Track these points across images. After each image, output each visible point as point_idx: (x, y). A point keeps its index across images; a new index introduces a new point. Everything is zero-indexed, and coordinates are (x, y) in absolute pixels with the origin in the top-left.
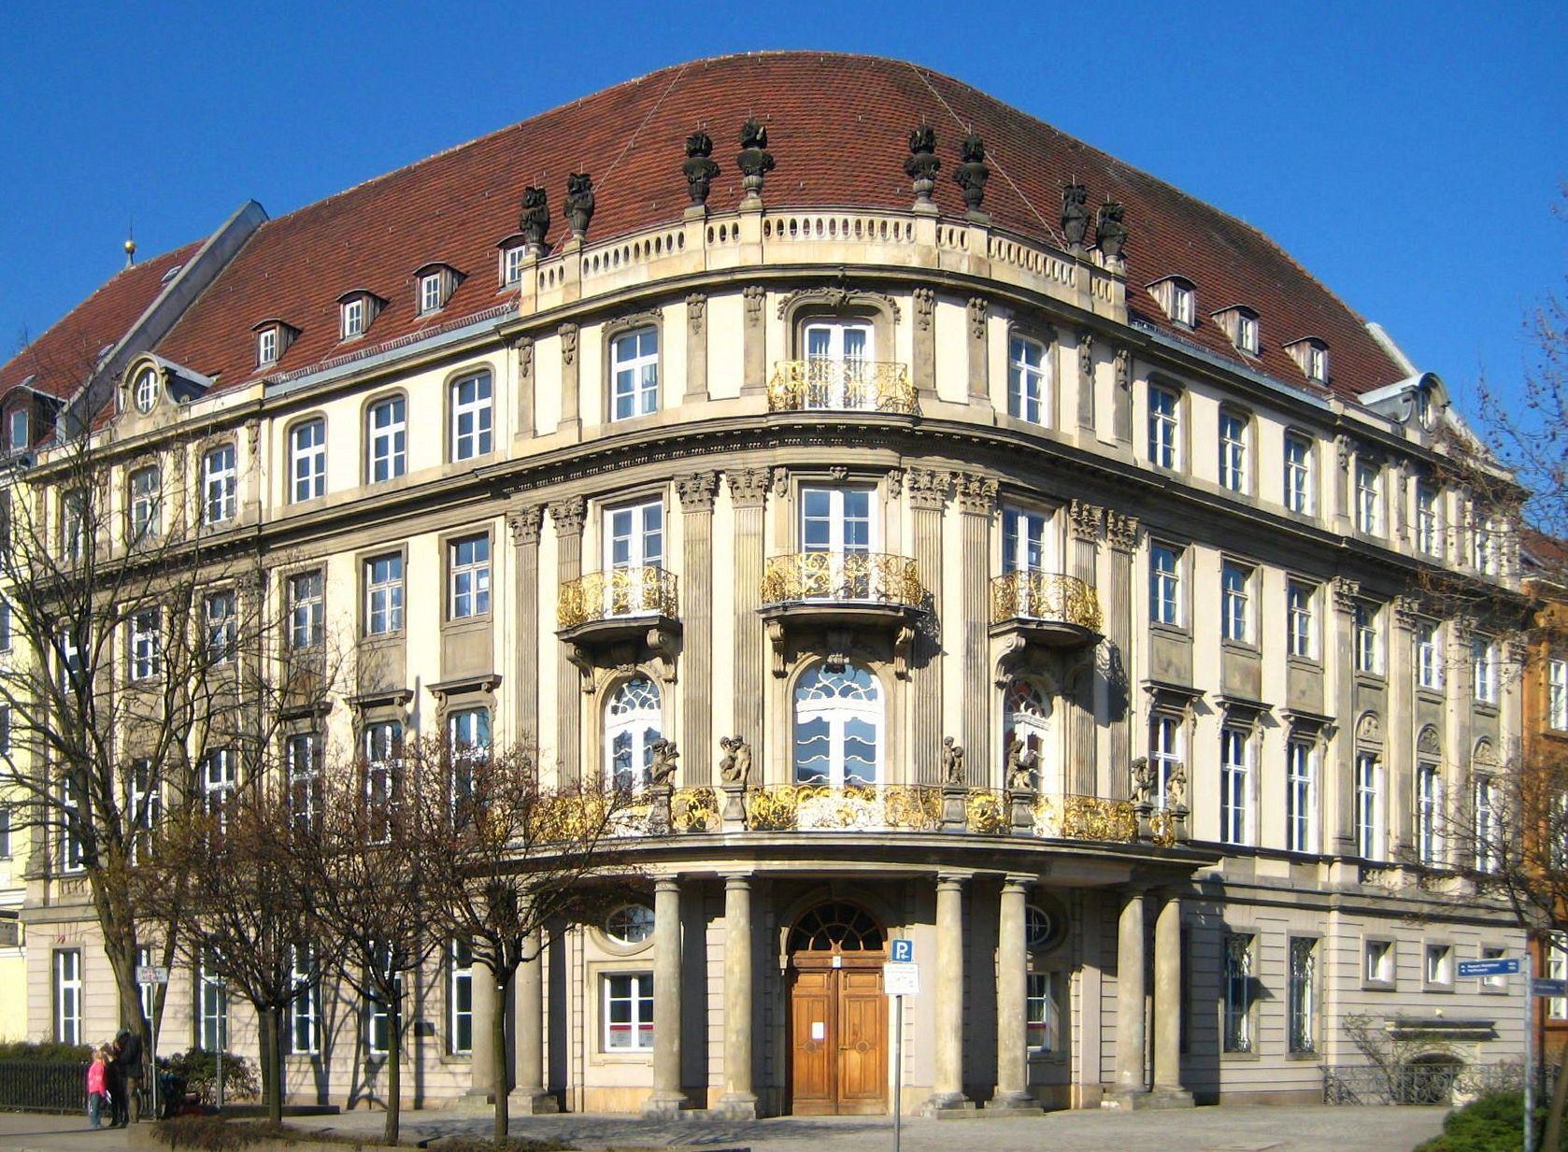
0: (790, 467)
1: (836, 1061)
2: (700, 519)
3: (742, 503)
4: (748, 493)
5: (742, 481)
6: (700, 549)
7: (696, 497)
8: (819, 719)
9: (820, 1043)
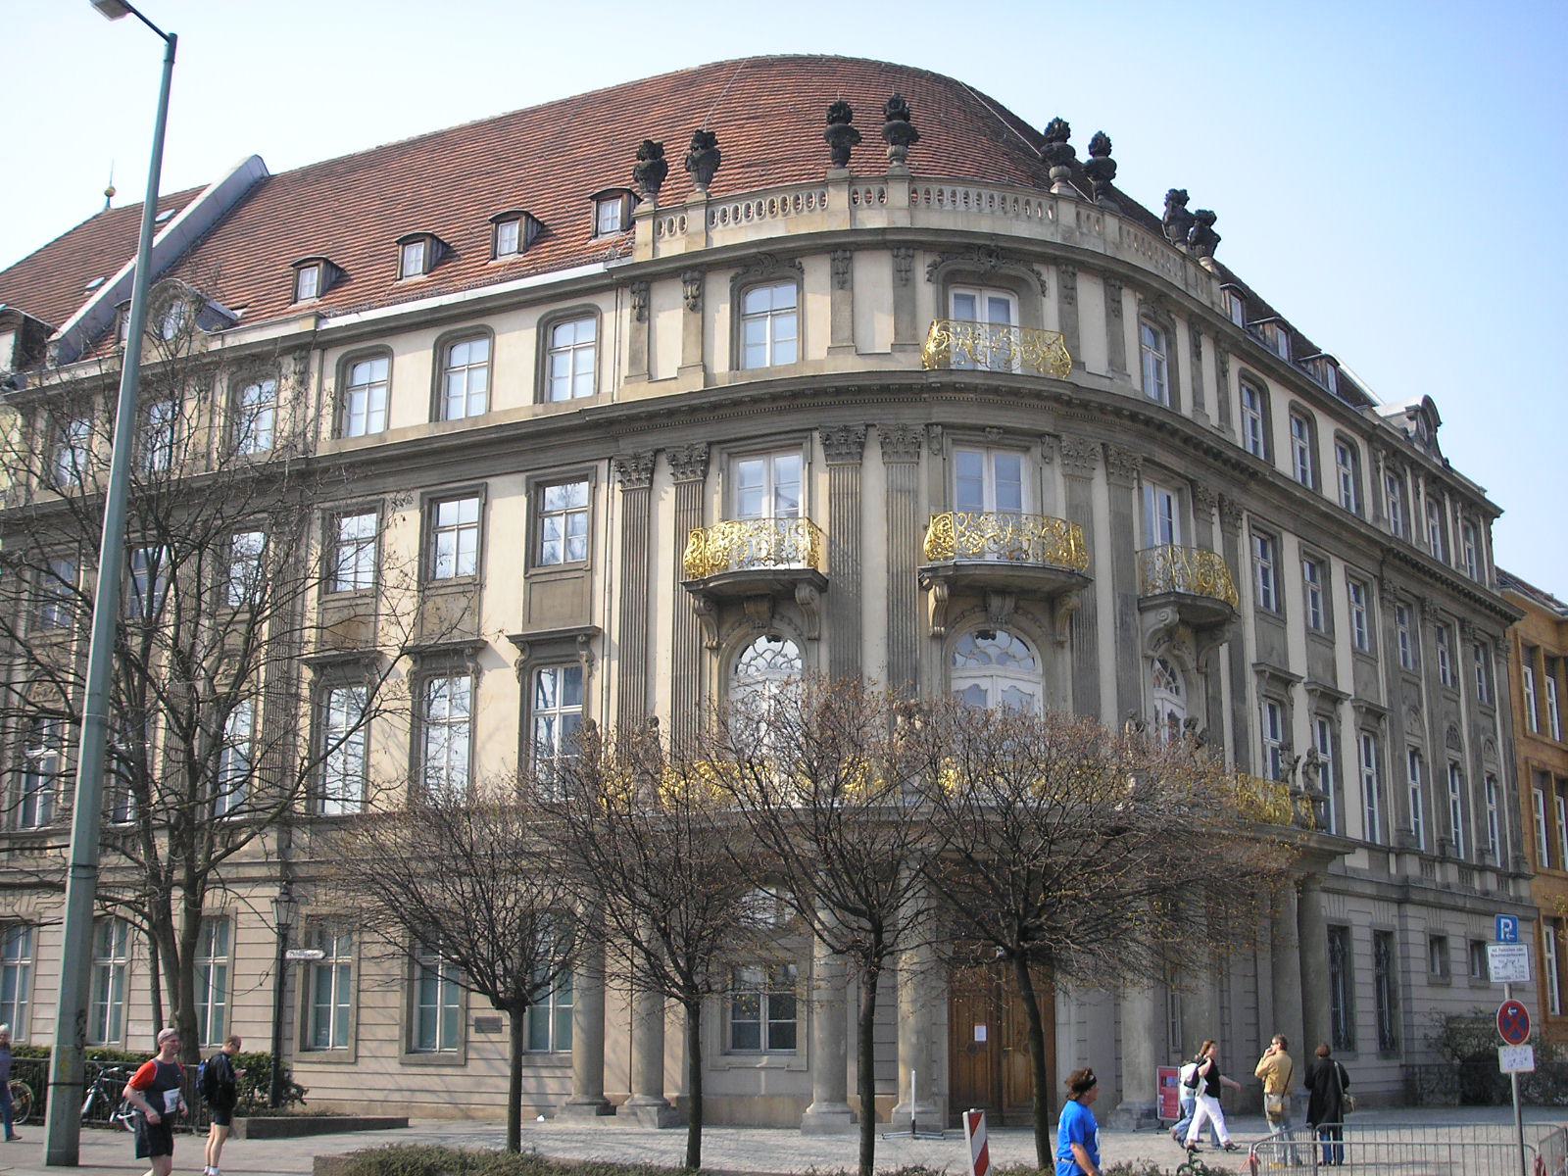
0: (944, 426)
1: (999, 1064)
2: (847, 477)
3: (895, 458)
4: (901, 448)
5: (895, 436)
6: (848, 503)
7: (844, 450)
8: (977, 686)
9: (981, 1043)
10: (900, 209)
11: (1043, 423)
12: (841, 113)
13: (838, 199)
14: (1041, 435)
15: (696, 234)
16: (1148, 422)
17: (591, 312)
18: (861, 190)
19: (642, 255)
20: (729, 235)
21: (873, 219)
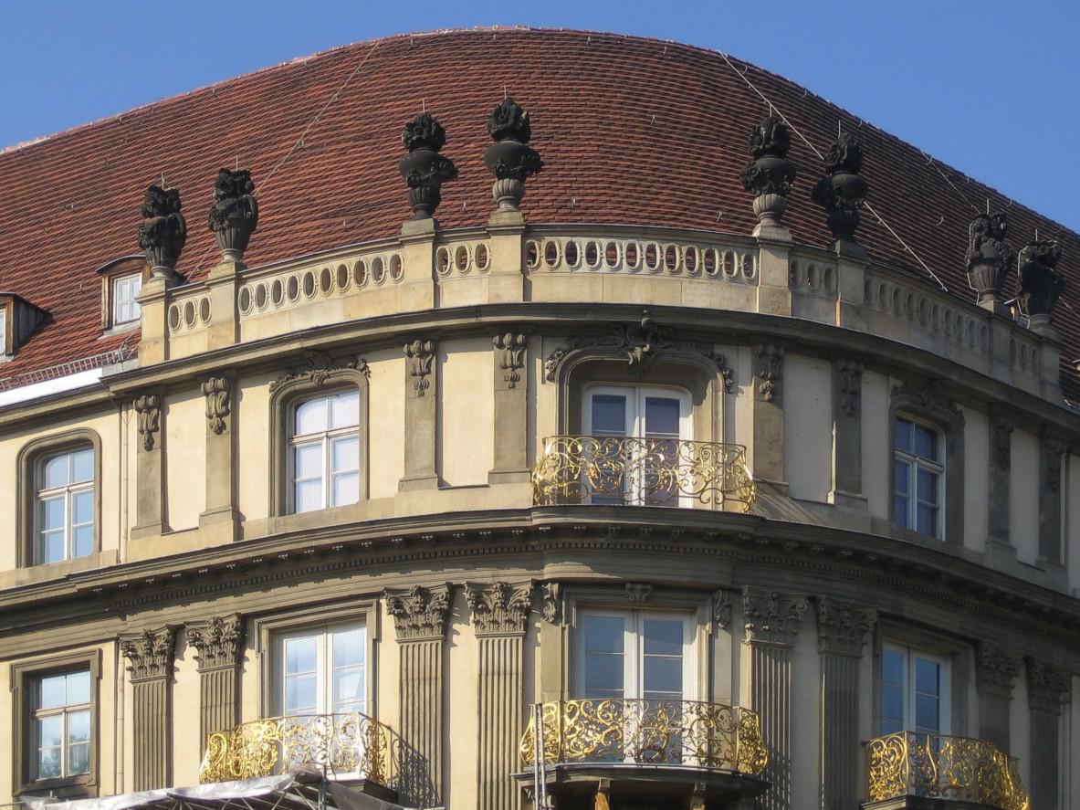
4: (500, 616)
10: (509, 274)
11: (712, 573)
12: (427, 136)
13: (418, 260)
14: (710, 590)
15: (222, 323)
16: (885, 563)
17: (83, 443)
18: (452, 249)
19: (150, 356)
20: (273, 322)
21: (466, 291)
